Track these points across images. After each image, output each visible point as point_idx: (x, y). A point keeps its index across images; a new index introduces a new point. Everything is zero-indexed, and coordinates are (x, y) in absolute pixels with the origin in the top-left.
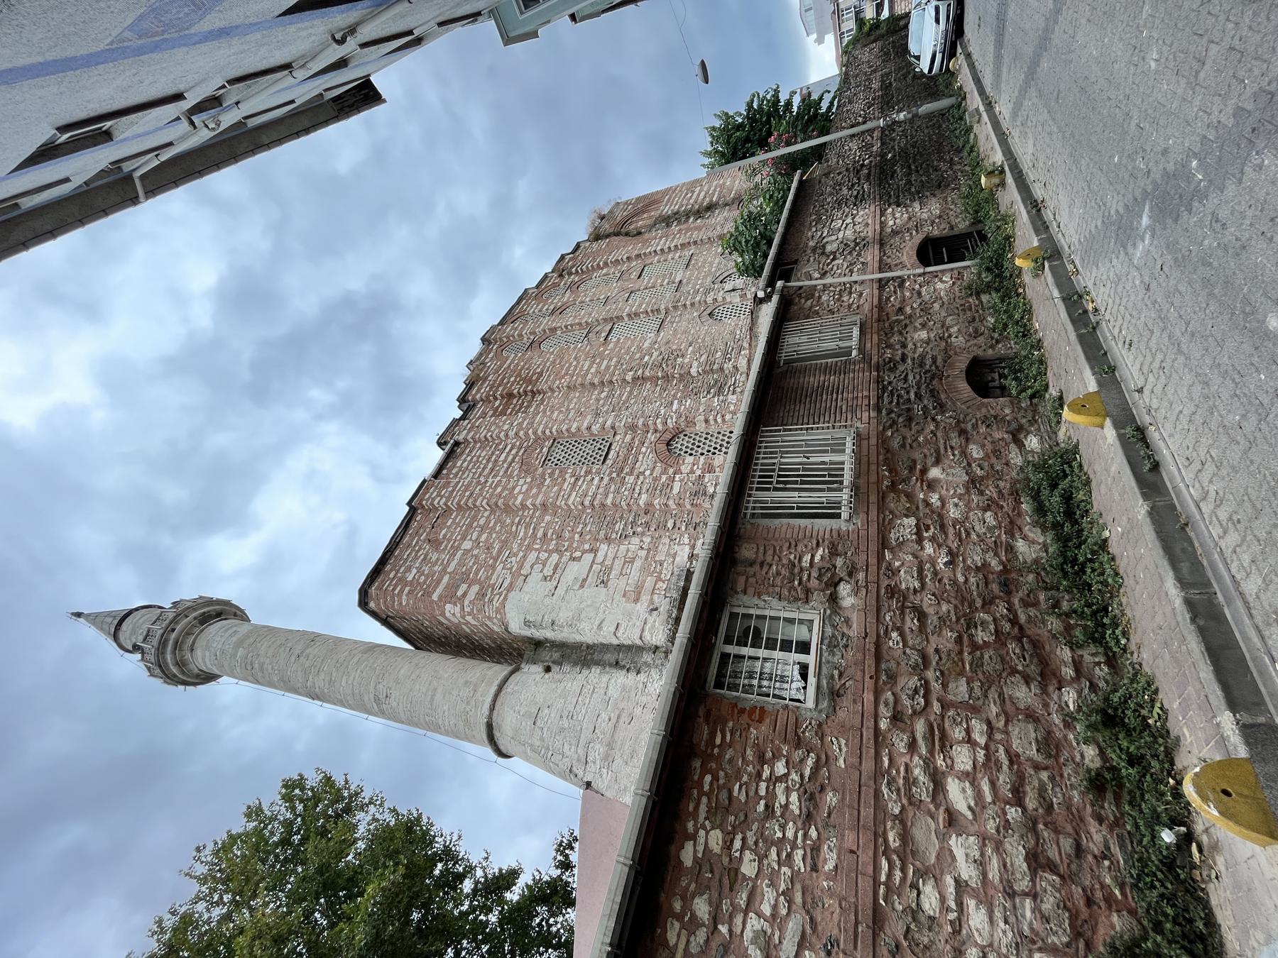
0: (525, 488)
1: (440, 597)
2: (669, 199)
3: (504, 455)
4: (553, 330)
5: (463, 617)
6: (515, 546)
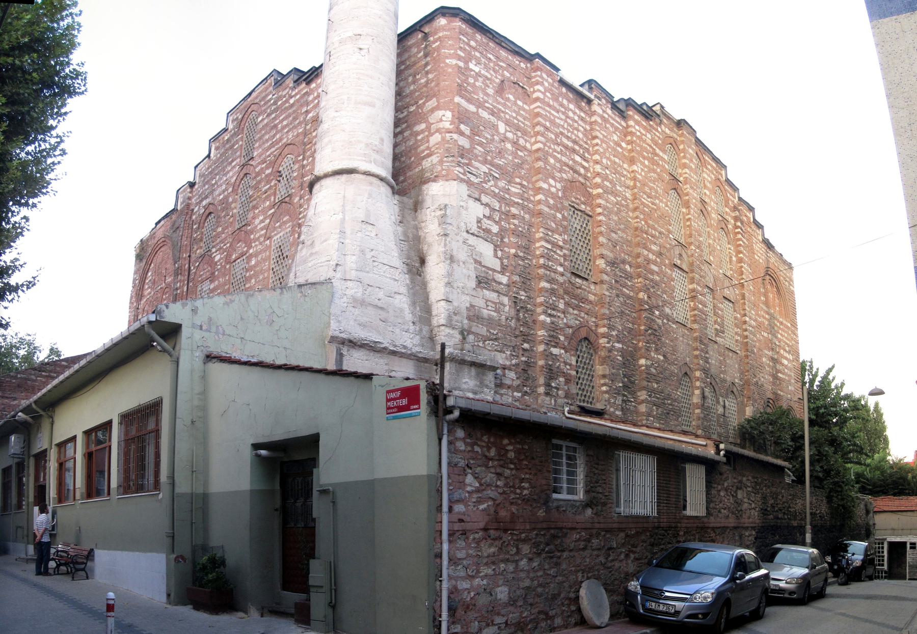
0: (553, 190)
3: (578, 159)
4: (687, 205)
5: (438, 131)
6: (502, 184)
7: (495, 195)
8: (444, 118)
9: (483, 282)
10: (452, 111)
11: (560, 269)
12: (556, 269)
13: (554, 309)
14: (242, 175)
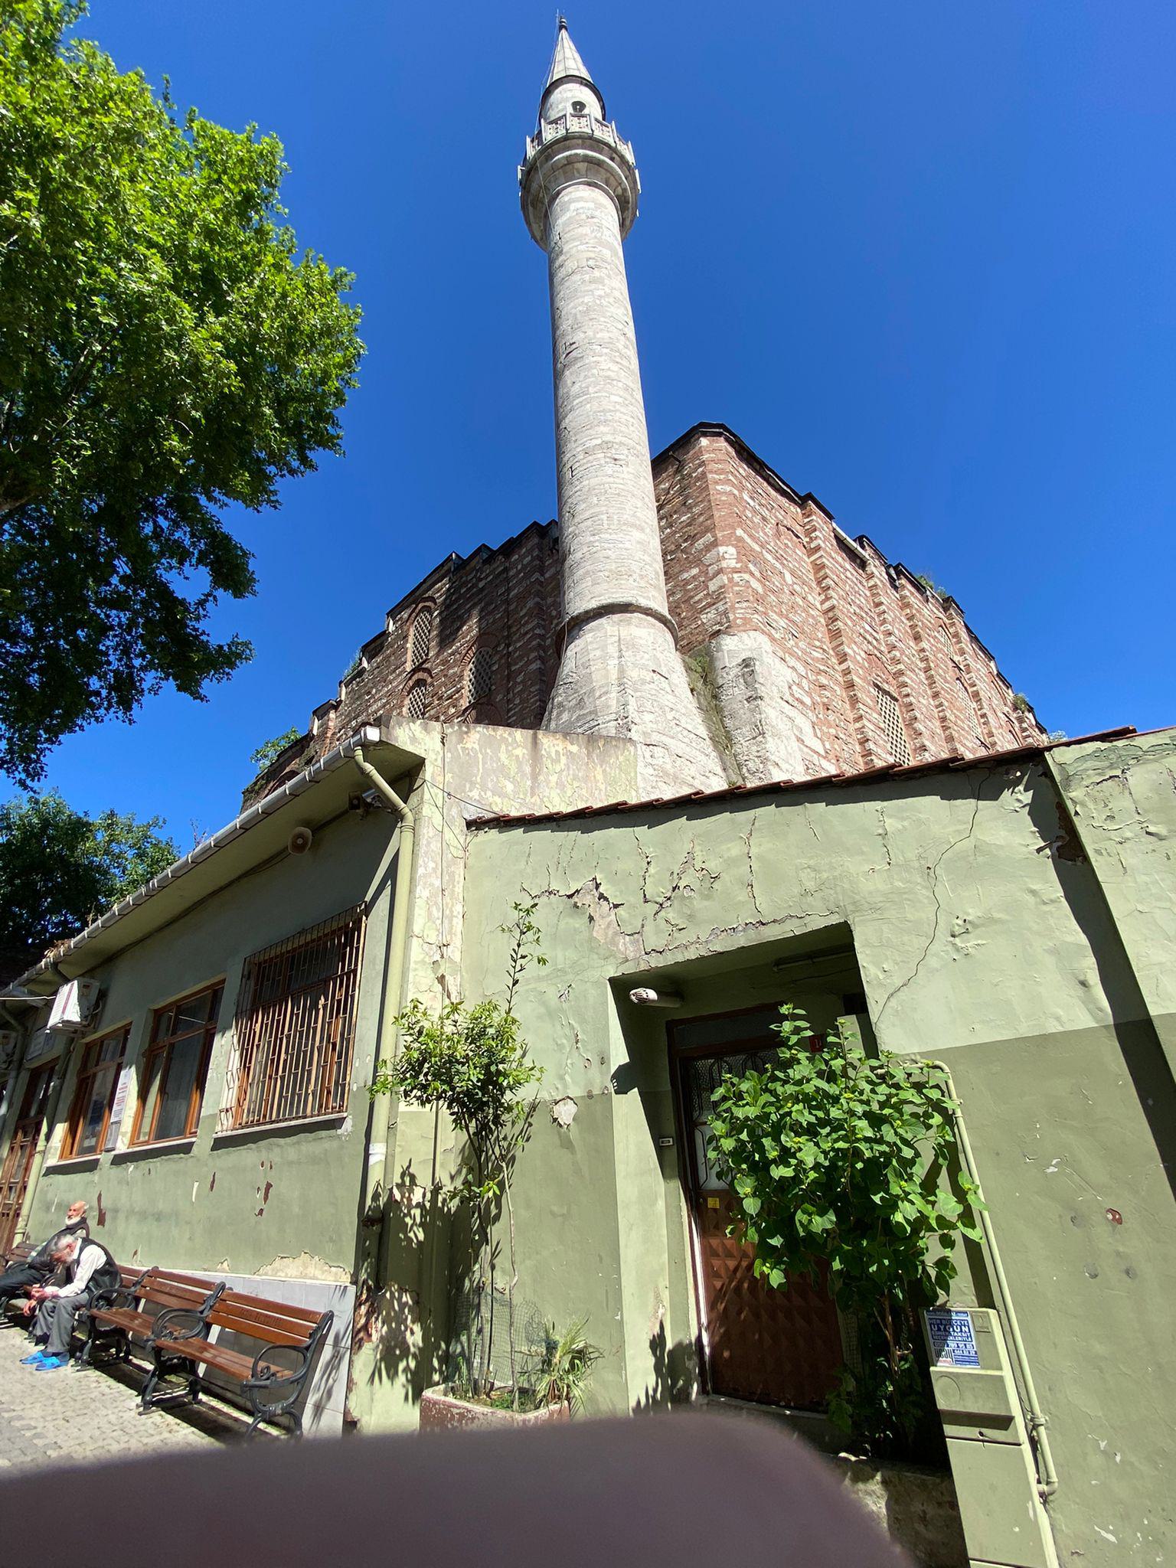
0: (858, 657)
1: (740, 539)
7: (798, 658)
8: (726, 556)
10: (736, 547)
14: (411, 683)
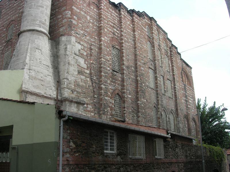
0: (106, 40)
2: (190, 89)
3: (115, 30)
6: (88, 38)
8: (68, 14)
9: (80, 72)
11: (108, 69)
12: (107, 69)
13: (106, 83)
